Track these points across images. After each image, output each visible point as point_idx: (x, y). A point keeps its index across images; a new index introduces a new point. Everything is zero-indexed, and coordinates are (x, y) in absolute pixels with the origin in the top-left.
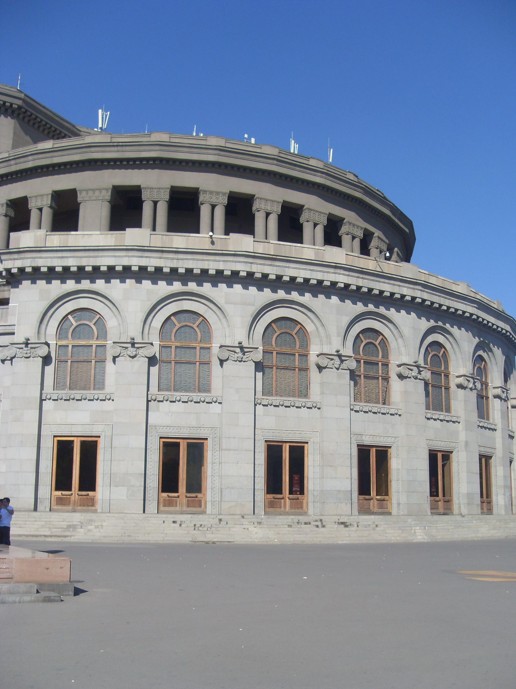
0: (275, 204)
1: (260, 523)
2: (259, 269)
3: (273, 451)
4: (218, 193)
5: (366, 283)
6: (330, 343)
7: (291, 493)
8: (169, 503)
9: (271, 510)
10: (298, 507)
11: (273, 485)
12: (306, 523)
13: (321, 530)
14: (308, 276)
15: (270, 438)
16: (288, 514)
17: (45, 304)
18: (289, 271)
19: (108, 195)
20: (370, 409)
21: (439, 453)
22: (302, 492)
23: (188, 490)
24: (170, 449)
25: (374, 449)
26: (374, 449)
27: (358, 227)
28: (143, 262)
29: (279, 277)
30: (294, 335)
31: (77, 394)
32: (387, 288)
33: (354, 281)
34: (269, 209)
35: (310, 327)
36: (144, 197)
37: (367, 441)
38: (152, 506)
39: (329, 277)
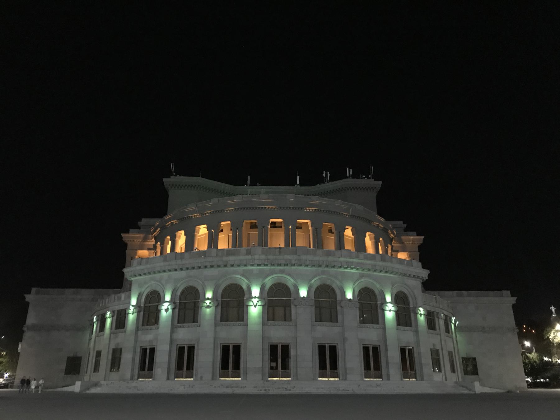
23: (188, 369)
31: (149, 327)
38: (172, 376)
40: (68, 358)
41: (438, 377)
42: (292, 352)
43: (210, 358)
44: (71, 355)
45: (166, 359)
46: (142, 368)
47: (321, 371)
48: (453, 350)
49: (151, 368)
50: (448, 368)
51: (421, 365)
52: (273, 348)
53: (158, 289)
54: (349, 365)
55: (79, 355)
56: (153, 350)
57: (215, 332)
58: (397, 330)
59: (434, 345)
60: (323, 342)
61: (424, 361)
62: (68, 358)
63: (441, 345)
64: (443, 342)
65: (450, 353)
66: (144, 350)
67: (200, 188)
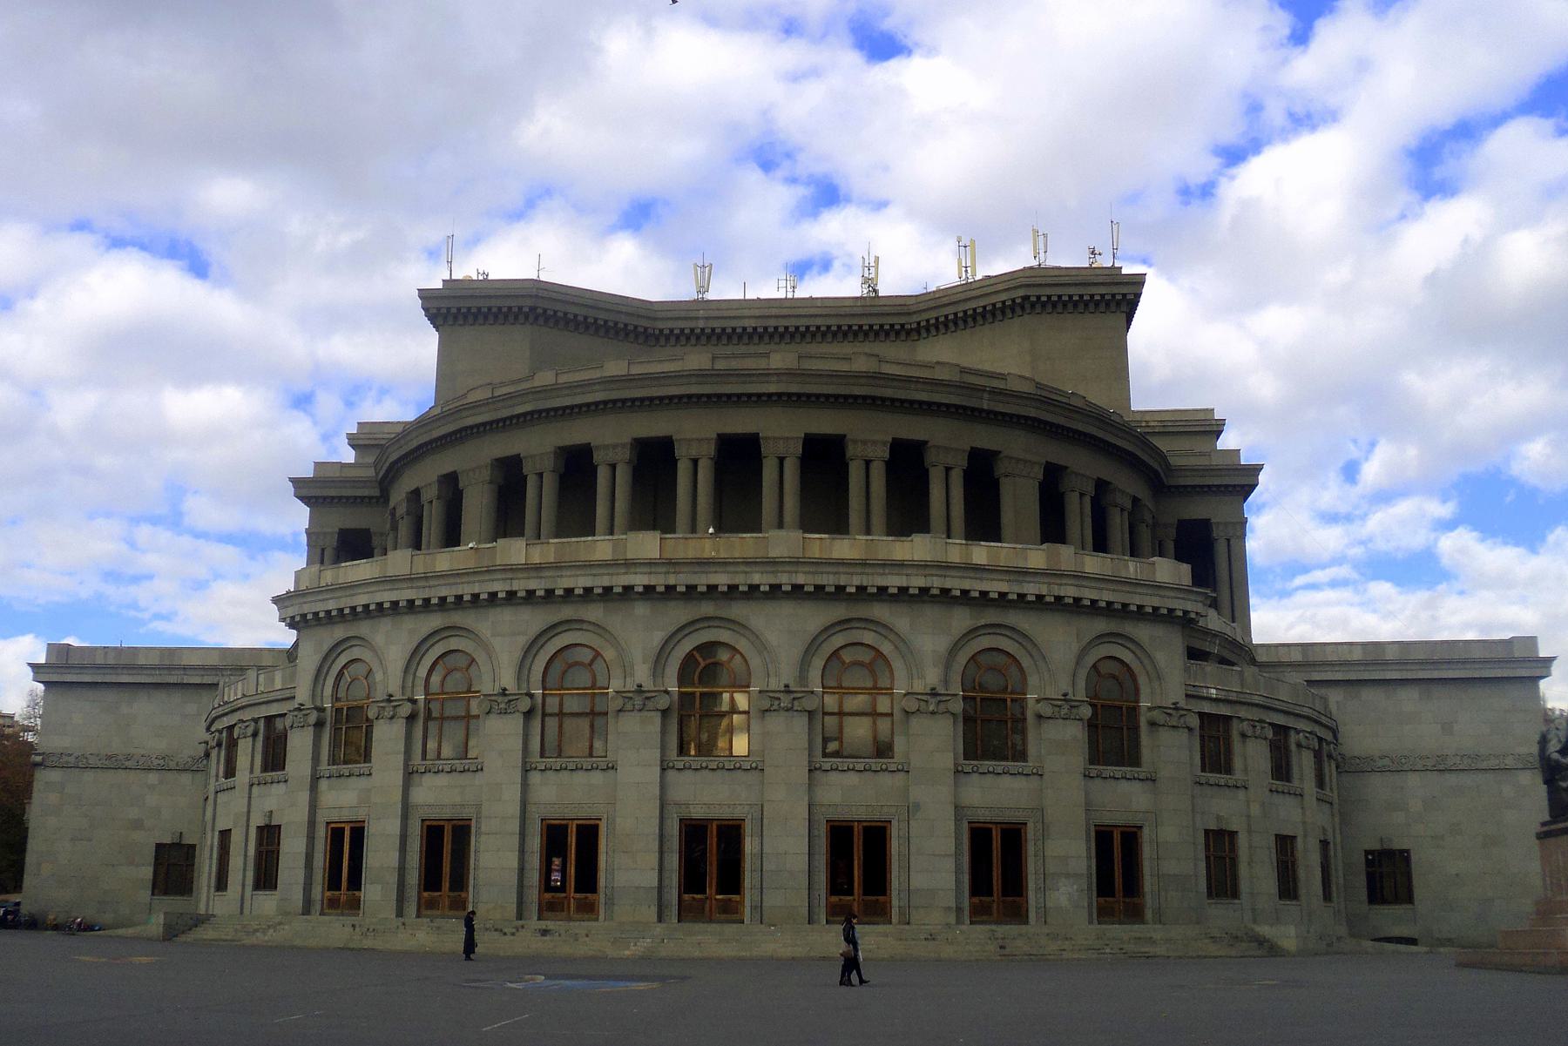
2: (521, 586)
4: (615, 446)
5: (680, 580)
6: (632, 675)
8: (432, 904)
10: (588, 909)
14: (589, 585)
17: (317, 658)
18: (563, 583)
19: (486, 474)
24: (433, 833)
27: (874, 443)
28: (394, 596)
29: (550, 593)
31: (345, 769)
32: (722, 580)
33: (659, 580)
34: (694, 453)
35: (609, 654)
36: (525, 471)
37: (698, 813)
38: (411, 908)
39: (620, 581)
40: (159, 846)
42: (749, 846)
43: (512, 861)
44: (167, 840)
45: (394, 857)
46: (333, 882)
47: (835, 899)
48: (1299, 833)
49: (355, 882)
52: (694, 831)
54: (918, 881)
55: (187, 841)
56: (358, 833)
57: (525, 785)
58: (1087, 776)
62: (159, 847)
65: (1285, 844)
66: (336, 834)
67: (536, 319)
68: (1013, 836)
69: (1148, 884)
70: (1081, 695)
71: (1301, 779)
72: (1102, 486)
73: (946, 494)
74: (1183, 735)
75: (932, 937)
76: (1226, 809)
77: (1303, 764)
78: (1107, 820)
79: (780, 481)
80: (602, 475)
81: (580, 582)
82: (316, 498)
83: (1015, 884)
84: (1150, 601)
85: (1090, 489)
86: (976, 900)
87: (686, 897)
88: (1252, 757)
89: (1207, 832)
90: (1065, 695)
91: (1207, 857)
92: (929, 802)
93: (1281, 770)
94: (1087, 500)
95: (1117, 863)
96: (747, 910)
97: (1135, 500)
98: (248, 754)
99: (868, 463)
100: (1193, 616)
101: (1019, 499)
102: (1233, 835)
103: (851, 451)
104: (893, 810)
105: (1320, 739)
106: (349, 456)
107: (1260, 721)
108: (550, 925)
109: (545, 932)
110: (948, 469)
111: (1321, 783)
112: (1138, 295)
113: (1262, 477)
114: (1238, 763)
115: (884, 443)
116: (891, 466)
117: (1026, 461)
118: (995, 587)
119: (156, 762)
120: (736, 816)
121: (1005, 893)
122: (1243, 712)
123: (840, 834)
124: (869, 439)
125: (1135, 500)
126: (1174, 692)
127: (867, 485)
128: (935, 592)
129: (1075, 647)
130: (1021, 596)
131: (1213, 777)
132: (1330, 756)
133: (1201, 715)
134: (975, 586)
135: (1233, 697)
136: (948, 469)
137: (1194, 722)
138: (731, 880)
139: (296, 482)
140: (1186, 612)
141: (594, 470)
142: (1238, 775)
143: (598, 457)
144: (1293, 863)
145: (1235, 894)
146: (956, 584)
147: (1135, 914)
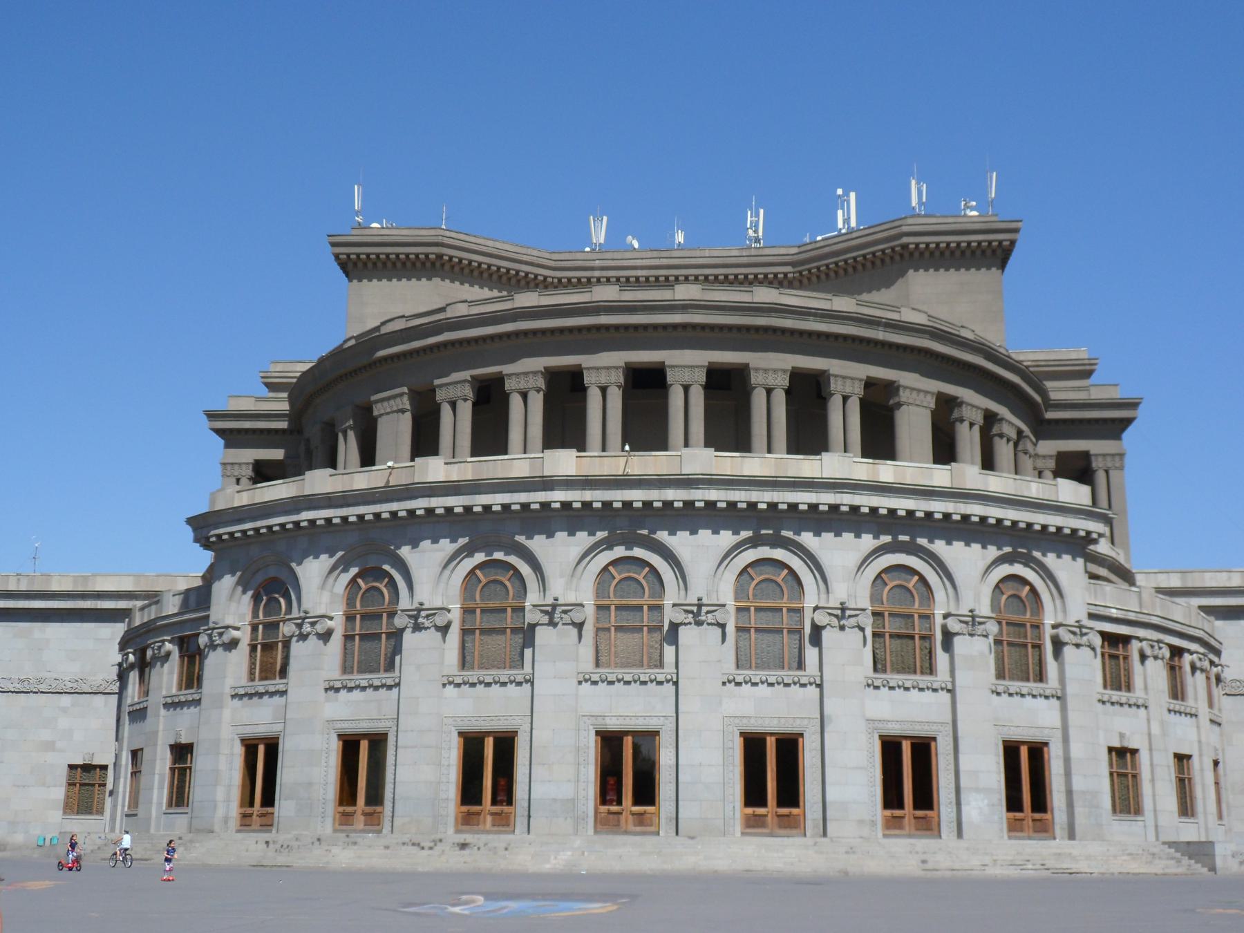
0: (613, 372)
1: (355, 843)
3: (472, 744)
7: (494, 802)
9: (465, 827)
11: (470, 792)
12: (413, 844)
13: (426, 852)
15: (465, 729)
16: (488, 832)
20: (620, 677)
21: (768, 738)
22: (510, 801)
25: (630, 738)
26: (630, 738)
27: (775, 371)
30: (507, 583)
34: (603, 379)
37: (613, 724)
41: (1125, 831)
42: (665, 758)
47: (750, 810)
50: (1169, 801)
51: (1069, 793)
53: (283, 575)
59: (1122, 736)
60: (756, 726)
61: (1078, 784)
63: (1149, 734)
64: (1156, 729)
68: (923, 749)
69: (1057, 798)
70: (984, 609)
71: (1196, 699)
72: (990, 418)
73: (843, 419)
74: (1086, 652)
75: (851, 851)
76: (1127, 727)
77: (1196, 684)
78: (1015, 735)
79: (686, 406)
80: (516, 402)
81: (497, 500)
82: (231, 431)
83: (925, 798)
84: (1054, 521)
85: (979, 418)
86: (888, 813)
87: (604, 808)
88: (1151, 677)
89: (1110, 750)
90: (971, 611)
91: (1111, 774)
92: (847, 713)
93: (1177, 691)
94: (976, 429)
95: (1027, 778)
96: (663, 821)
97: (1020, 432)
98: (167, 678)
99: (769, 391)
100: (1095, 536)
101: (914, 424)
102: (1134, 752)
103: (756, 378)
104: (806, 722)
105: (1212, 663)
106: (264, 392)
107: (1159, 641)
108: (468, 838)
109: (463, 846)
110: (845, 399)
111: (1211, 705)
112: (1013, 243)
113: (1141, 413)
114: (1138, 681)
115: (784, 371)
116: (788, 392)
117: (919, 391)
118: (903, 504)
119: (70, 685)
120: (651, 728)
121: (917, 806)
122: (1141, 633)
123: (753, 745)
124: (771, 369)
125: (1020, 432)
126: (1077, 612)
127: (769, 411)
128: (844, 509)
129: (982, 565)
130: (929, 515)
131: (1116, 695)
132: (1218, 679)
133: (1105, 636)
134: (884, 503)
135: (1132, 616)
136: (845, 399)
137: (1097, 641)
138: (646, 792)
139: (212, 416)
140: (1089, 533)
141: (505, 398)
142: (1138, 694)
143: (509, 385)
144: (1190, 779)
145: (1138, 811)
146: (865, 501)
147: (1044, 829)
